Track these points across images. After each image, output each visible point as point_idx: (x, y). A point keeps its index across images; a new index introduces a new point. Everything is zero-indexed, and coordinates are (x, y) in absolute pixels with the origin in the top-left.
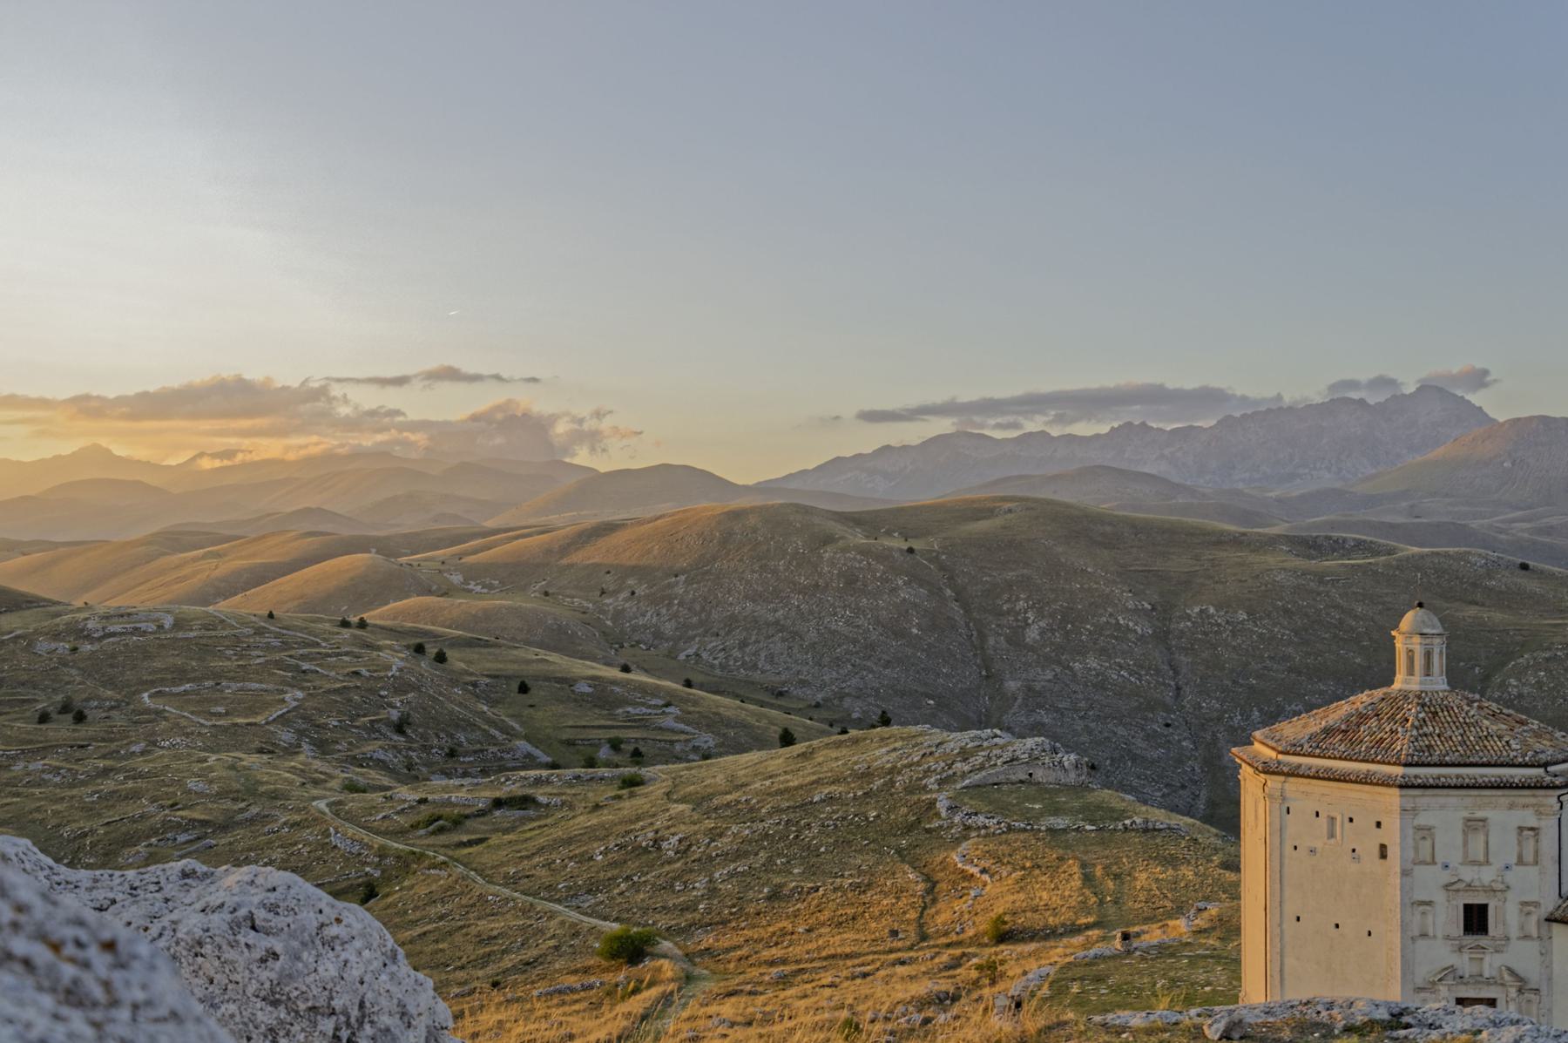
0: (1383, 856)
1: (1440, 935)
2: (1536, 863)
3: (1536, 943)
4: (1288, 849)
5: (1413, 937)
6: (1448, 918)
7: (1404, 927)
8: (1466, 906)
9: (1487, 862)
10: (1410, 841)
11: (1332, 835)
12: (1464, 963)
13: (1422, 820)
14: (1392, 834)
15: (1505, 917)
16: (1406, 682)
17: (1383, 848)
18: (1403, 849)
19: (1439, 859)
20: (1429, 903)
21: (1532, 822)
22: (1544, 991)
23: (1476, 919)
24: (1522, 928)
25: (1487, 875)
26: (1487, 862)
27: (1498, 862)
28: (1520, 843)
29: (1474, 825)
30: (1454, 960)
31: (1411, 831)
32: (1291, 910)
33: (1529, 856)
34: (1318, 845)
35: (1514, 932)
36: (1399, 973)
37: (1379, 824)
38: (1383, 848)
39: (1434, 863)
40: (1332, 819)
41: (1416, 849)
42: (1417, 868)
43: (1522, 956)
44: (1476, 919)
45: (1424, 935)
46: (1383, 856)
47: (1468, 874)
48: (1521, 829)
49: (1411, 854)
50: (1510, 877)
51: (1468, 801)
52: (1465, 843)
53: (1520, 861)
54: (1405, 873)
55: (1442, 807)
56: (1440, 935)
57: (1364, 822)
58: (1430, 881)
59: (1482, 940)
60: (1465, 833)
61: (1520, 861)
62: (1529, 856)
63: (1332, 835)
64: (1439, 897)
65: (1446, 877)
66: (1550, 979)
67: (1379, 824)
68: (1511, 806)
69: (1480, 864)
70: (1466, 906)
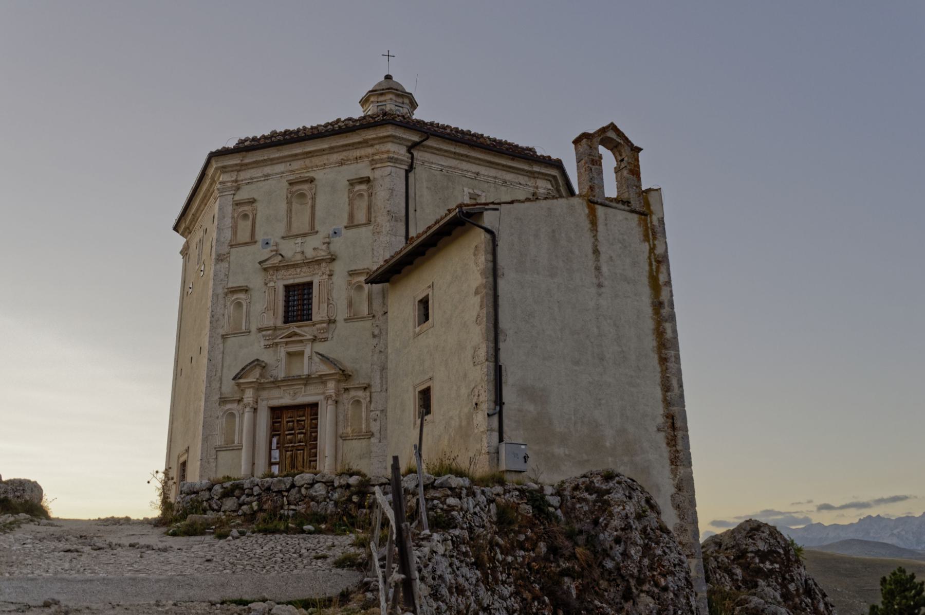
1: (253, 329)
2: (369, 222)
3: (368, 324)
6: (265, 306)
7: (214, 321)
8: (287, 288)
9: (313, 232)
10: (228, 221)
12: (276, 360)
13: (243, 195)
15: (334, 294)
18: (219, 229)
19: (260, 236)
20: (246, 290)
21: (366, 172)
22: (376, 387)
23: (298, 303)
24: (350, 305)
25: (312, 247)
26: (313, 232)
27: (324, 230)
28: (351, 203)
29: (301, 188)
30: (267, 357)
31: (229, 209)
33: (361, 217)
35: (341, 313)
36: (204, 377)
39: (253, 242)
41: (235, 229)
42: (233, 250)
43: (347, 344)
44: (298, 303)
45: (237, 333)
47: (290, 250)
48: (352, 183)
49: (228, 234)
50: (338, 245)
51: (296, 165)
52: (289, 211)
53: (352, 225)
54: (220, 258)
55: (267, 177)
56: (253, 329)
58: (247, 261)
59: (307, 331)
60: (289, 203)
61: (352, 225)
62: (361, 217)
64: (256, 281)
65: (266, 253)
66: (383, 369)
68: (342, 163)
69: (305, 235)
70: (287, 288)
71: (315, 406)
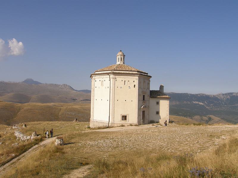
0: (134, 87)
4: (116, 87)
5: (139, 101)
11: (125, 84)
14: (136, 83)
16: (120, 63)
17: (135, 85)
28: (148, 86)
32: (116, 100)
34: (122, 86)
37: (134, 81)
38: (135, 85)
40: (125, 81)
46: (134, 87)
54: (138, 90)
57: (131, 81)
63: (125, 84)
67: (134, 81)
71: (144, 111)
